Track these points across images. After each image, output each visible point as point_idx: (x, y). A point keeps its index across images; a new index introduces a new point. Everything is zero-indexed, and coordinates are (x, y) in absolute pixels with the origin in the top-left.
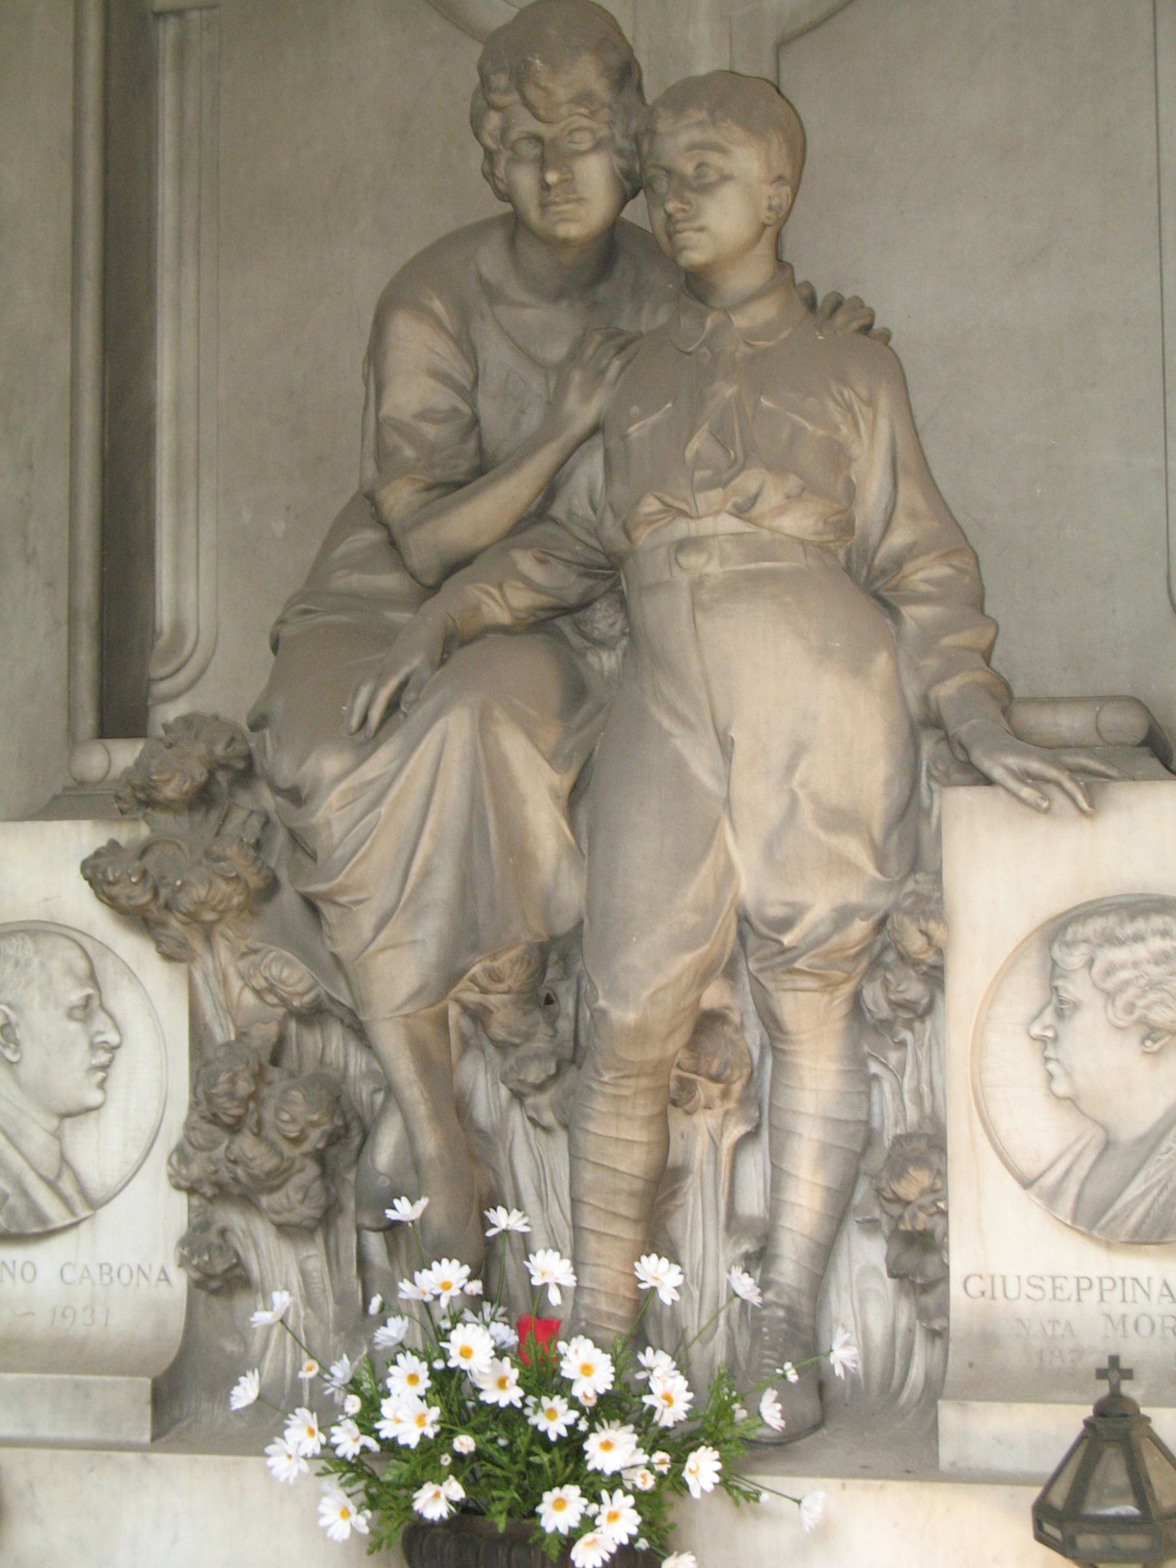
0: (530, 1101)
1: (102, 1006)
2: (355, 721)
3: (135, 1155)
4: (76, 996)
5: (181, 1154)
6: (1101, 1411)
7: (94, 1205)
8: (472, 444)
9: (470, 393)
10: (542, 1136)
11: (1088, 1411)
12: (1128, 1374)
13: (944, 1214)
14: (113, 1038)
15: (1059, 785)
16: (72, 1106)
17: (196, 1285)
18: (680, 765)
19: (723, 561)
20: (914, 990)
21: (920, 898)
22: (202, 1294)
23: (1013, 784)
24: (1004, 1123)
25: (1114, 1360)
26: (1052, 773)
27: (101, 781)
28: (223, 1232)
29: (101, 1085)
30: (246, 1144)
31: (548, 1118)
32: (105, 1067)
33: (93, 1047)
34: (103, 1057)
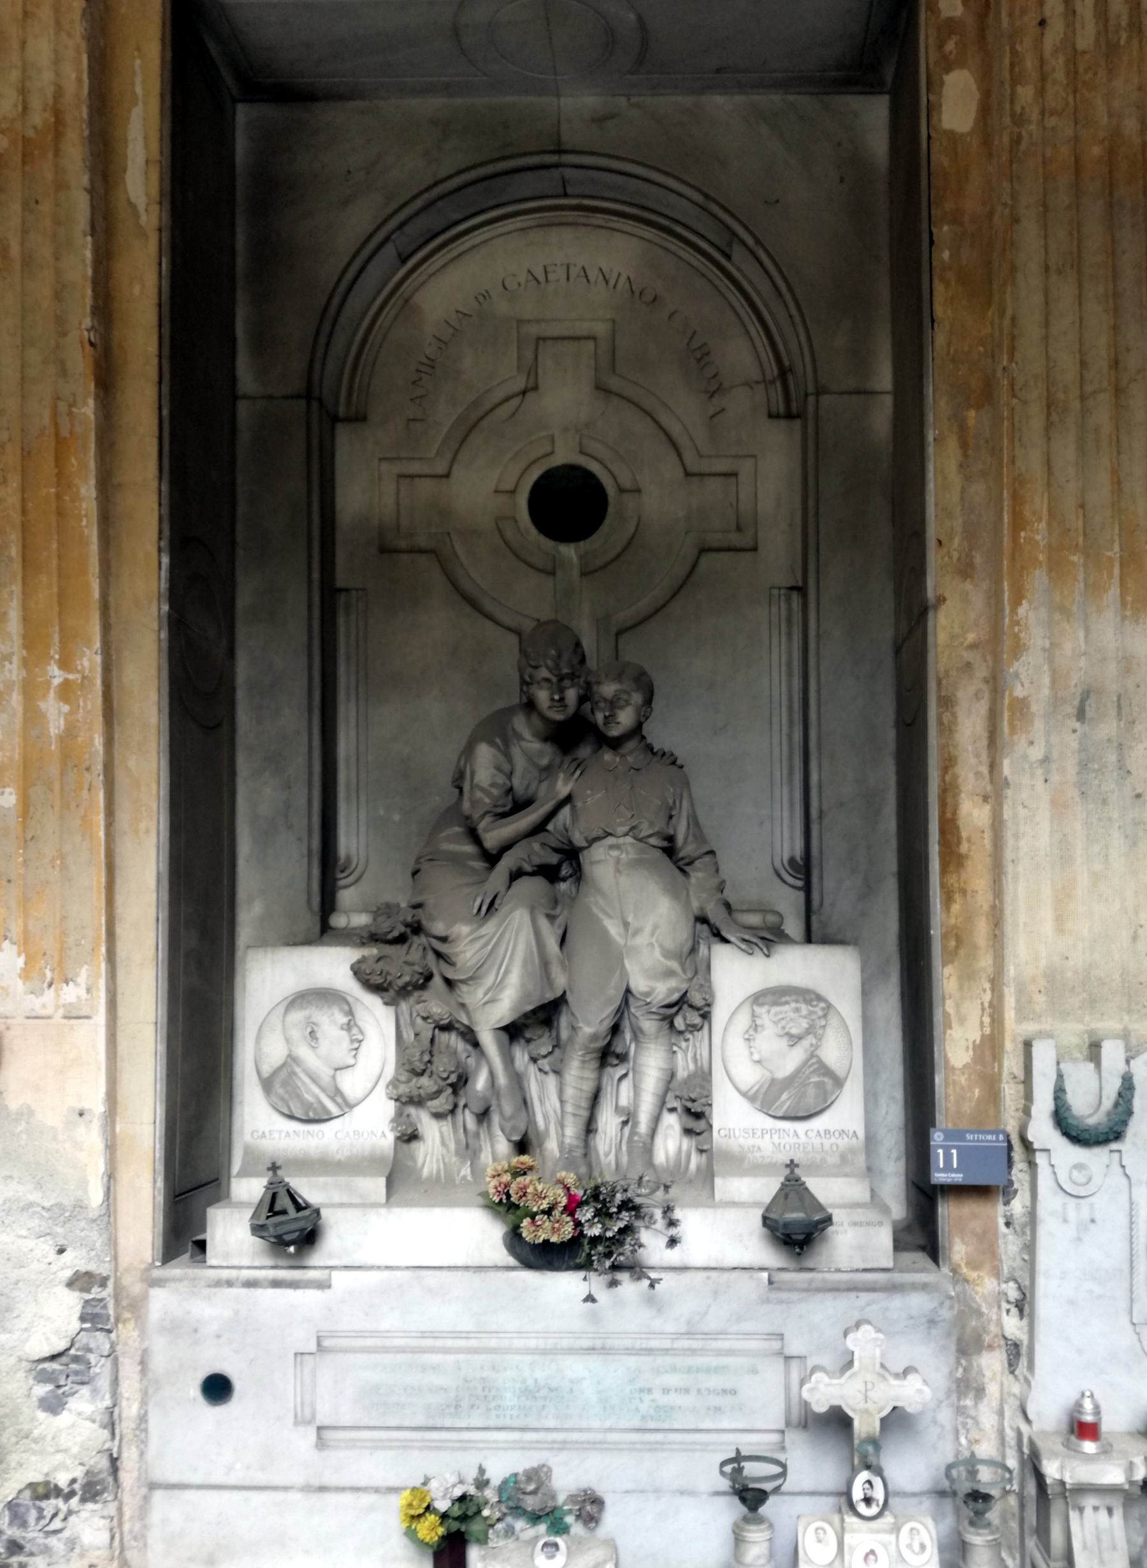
0: (540, 1062)
1: (356, 1025)
2: (475, 911)
3: (370, 1085)
4: (345, 1020)
5: (394, 1083)
6: (787, 1179)
7: (351, 1106)
8: (510, 798)
9: (510, 775)
10: (543, 1076)
11: (782, 1179)
12: (797, 1166)
13: (711, 1105)
14: (360, 1037)
15: (756, 945)
16: (342, 1065)
17: (398, 1139)
18: (605, 932)
19: (627, 853)
20: (697, 1020)
21: (701, 986)
22: (399, 1143)
23: (739, 943)
24: (733, 1071)
25: (792, 1161)
26: (754, 940)
27: (344, 929)
28: (408, 1116)
29: (355, 1056)
30: (424, 1081)
31: (547, 1068)
32: (357, 1049)
33: (352, 1041)
34: (356, 1045)
